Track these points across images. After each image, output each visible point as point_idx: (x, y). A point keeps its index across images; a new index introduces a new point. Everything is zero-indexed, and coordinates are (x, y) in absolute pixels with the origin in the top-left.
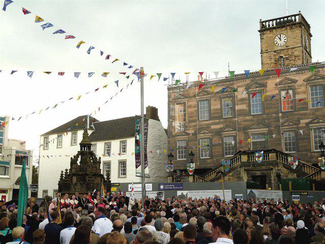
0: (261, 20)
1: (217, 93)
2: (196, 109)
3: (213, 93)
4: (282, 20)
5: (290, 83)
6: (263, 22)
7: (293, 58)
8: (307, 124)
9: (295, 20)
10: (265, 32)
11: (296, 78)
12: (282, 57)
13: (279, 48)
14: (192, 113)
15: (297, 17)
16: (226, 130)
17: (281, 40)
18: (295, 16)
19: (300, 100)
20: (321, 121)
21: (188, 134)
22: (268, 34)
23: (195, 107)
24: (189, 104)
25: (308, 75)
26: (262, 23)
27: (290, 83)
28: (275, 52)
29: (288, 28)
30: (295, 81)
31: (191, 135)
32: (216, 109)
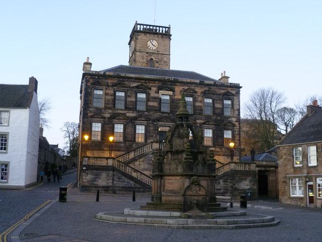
0: (136, 22)
1: (133, 87)
2: (113, 97)
3: (129, 87)
4: (155, 28)
5: (192, 92)
6: (139, 24)
7: (162, 63)
8: (201, 124)
9: (159, 31)
10: (139, 34)
11: (197, 89)
12: (152, 59)
13: (151, 51)
14: (109, 100)
15: (167, 29)
16: (139, 119)
17: (153, 44)
18: (166, 27)
19: (199, 106)
20: (211, 123)
21: (104, 118)
22: (141, 37)
23: (111, 96)
24: (107, 91)
25: (202, 90)
26: (137, 24)
27: (192, 92)
28: (147, 53)
29: (160, 36)
30: (196, 92)
31: (107, 119)
32: (131, 101)
